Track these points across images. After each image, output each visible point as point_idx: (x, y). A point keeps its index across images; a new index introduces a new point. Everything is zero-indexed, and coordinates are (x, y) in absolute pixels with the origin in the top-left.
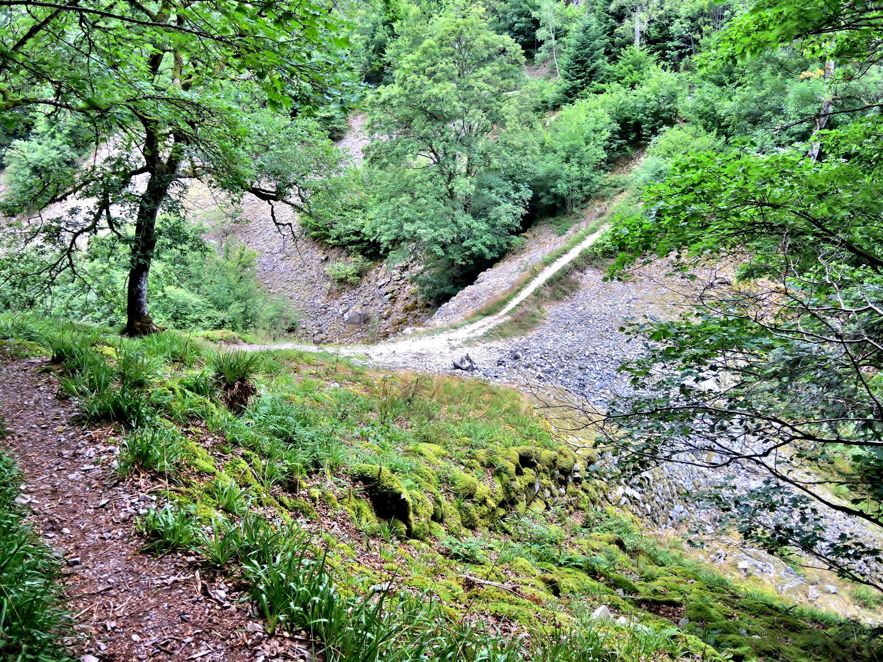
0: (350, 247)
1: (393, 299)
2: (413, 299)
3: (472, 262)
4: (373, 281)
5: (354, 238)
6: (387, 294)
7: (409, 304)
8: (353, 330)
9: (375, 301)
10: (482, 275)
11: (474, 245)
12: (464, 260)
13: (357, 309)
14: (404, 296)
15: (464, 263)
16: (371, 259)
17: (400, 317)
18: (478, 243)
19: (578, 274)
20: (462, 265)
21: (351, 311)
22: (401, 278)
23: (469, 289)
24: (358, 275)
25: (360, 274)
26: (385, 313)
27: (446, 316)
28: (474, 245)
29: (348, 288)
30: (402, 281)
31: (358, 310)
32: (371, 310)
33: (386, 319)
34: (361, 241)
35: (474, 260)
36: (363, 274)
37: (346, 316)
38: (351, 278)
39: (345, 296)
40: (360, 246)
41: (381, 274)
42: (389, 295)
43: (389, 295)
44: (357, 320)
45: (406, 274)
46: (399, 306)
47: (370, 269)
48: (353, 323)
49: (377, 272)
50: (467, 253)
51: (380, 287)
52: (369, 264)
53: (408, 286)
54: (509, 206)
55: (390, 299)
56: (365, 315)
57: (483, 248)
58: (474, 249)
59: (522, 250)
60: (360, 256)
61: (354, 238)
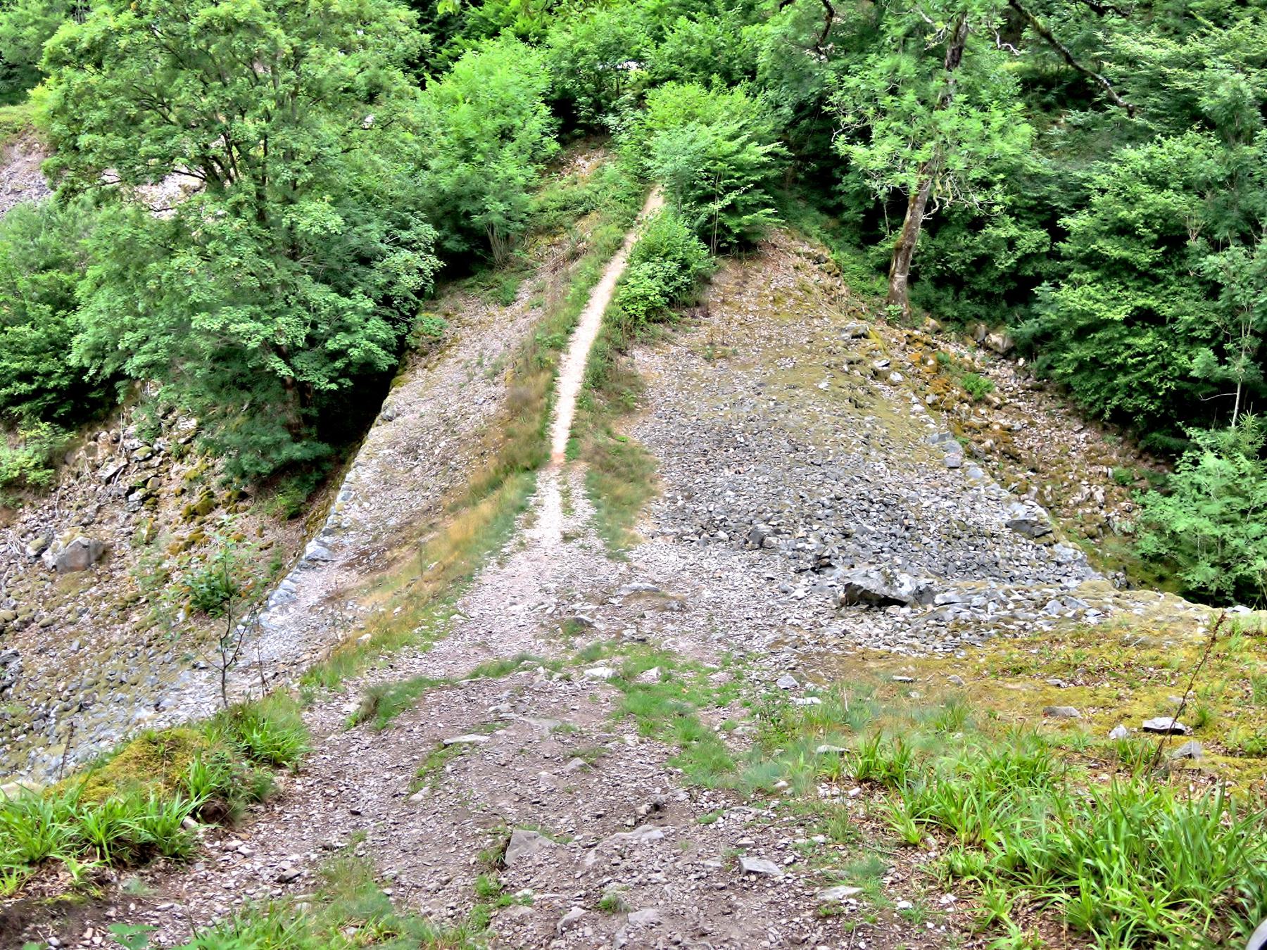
0: (14, 410)
1: (152, 500)
2: (199, 489)
3: (348, 383)
4: (87, 470)
5: (24, 387)
6: (132, 490)
7: (196, 501)
8: (75, 585)
9: (108, 511)
10: (394, 400)
11: (351, 346)
12: (332, 380)
13: (69, 538)
14: (174, 487)
15: (334, 386)
16: (69, 428)
17: (186, 532)
18: (359, 337)
19: (624, 359)
20: (330, 391)
21: (59, 543)
22: (154, 453)
23: (377, 434)
24: (48, 465)
25: (52, 462)
26: (145, 532)
27: (366, 498)
28: (351, 346)
29: (30, 498)
30: (156, 461)
31: (80, 538)
32: (105, 533)
33: (148, 544)
34: (39, 393)
35: (352, 378)
36: (56, 460)
37: (48, 557)
38: (33, 476)
39: (27, 514)
40: (39, 403)
41: (102, 452)
42: (139, 493)
43: (139, 493)
44: (82, 560)
45: (160, 443)
46: (171, 510)
47: (71, 448)
48: (72, 569)
49: (91, 451)
50: (339, 364)
51: (108, 481)
52: (67, 437)
53: (177, 467)
54: (406, 254)
55: (144, 500)
56: (97, 545)
57: (374, 347)
58: (355, 353)
59: (438, 344)
60: (44, 426)
61: (24, 387)
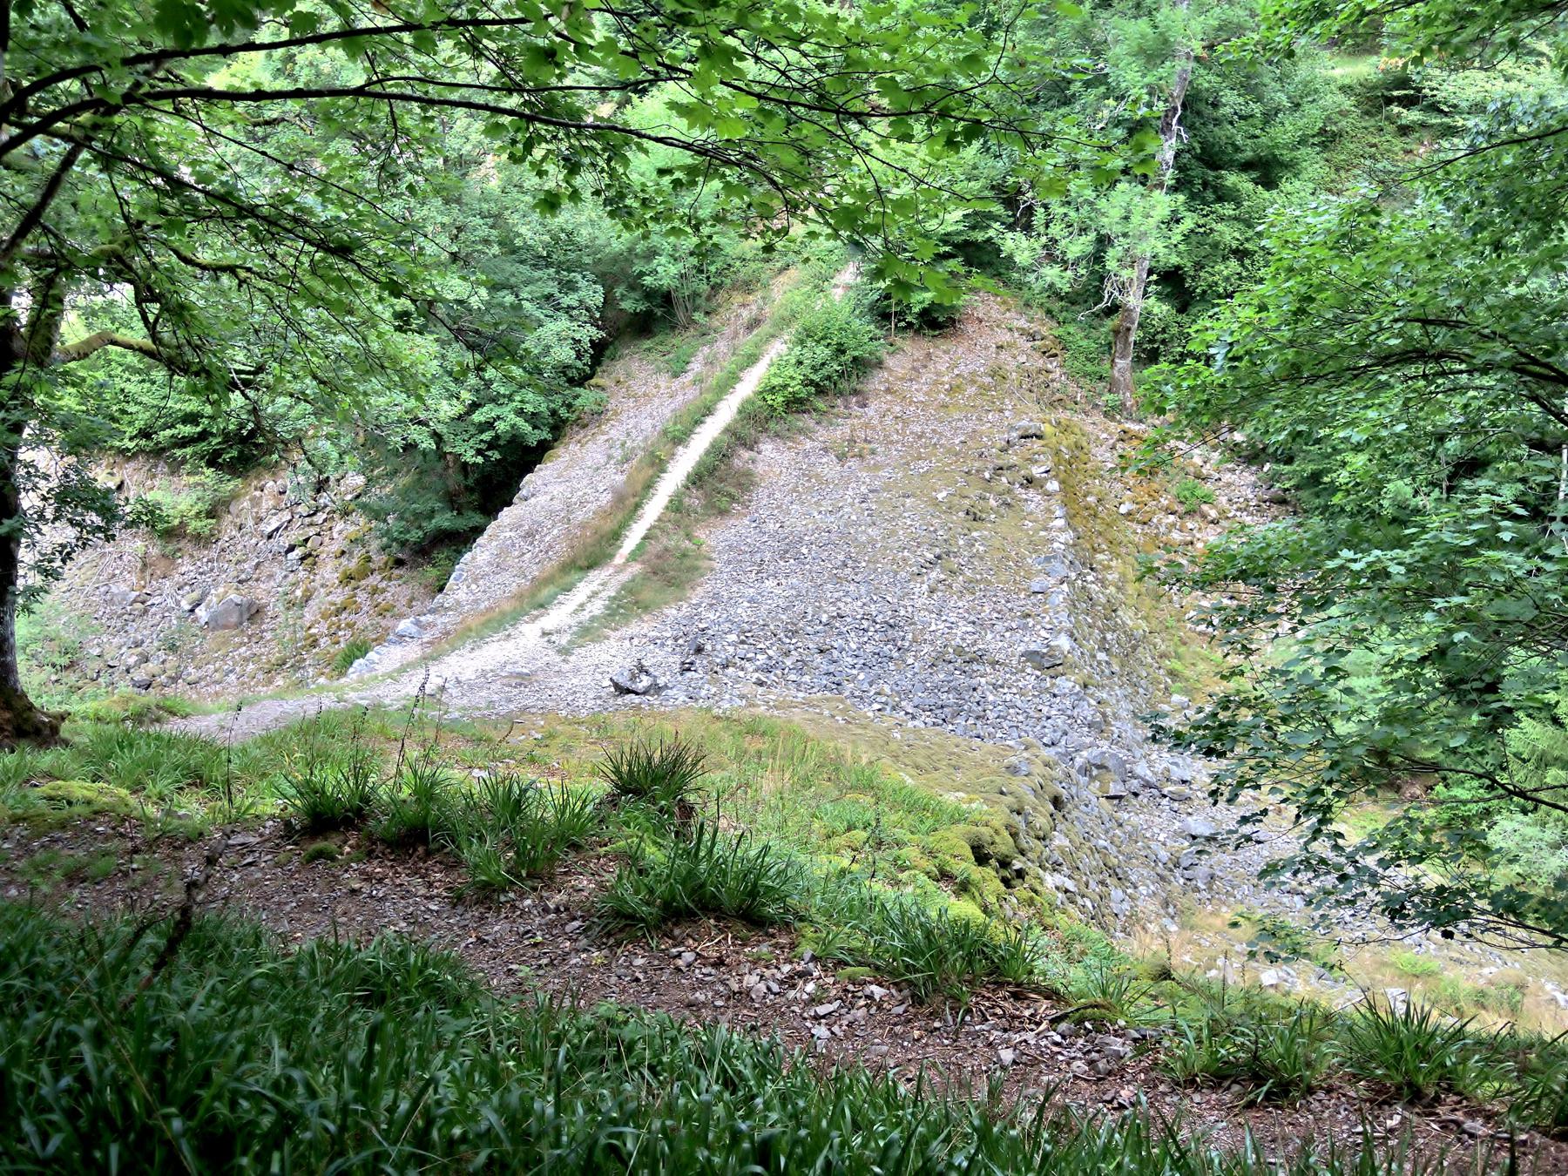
0: (178, 452)
2: (359, 552)
4: (251, 523)
6: (291, 549)
7: (352, 564)
9: (266, 569)
10: (530, 481)
12: (479, 452)
13: (224, 594)
14: (335, 548)
15: (480, 460)
17: (339, 597)
19: (746, 454)
21: (213, 599)
23: (506, 515)
24: (211, 514)
26: (299, 593)
27: (475, 581)
32: (261, 592)
34: (204, 436)
36: (220, 508)
37: (201, 612)
38: (194, 525)
39: (186, 566)
41: (268, 503)
42: (298, 552)
43: (298, 552)
44: (234, 619)
45: (324, 499)
46: (329, 571)
47: (235, 496)
48: (225, 627)
49: (256, 502)
50: (486, 436)
51: (270, 537)
52: (231, 485)
53: (340, 525)
54: (563, 323)
55: (303, 559)
56: (251, 605)
57: (520, 421)
58: (501, 426)
60: (209, 471)
61: (187, 430)
